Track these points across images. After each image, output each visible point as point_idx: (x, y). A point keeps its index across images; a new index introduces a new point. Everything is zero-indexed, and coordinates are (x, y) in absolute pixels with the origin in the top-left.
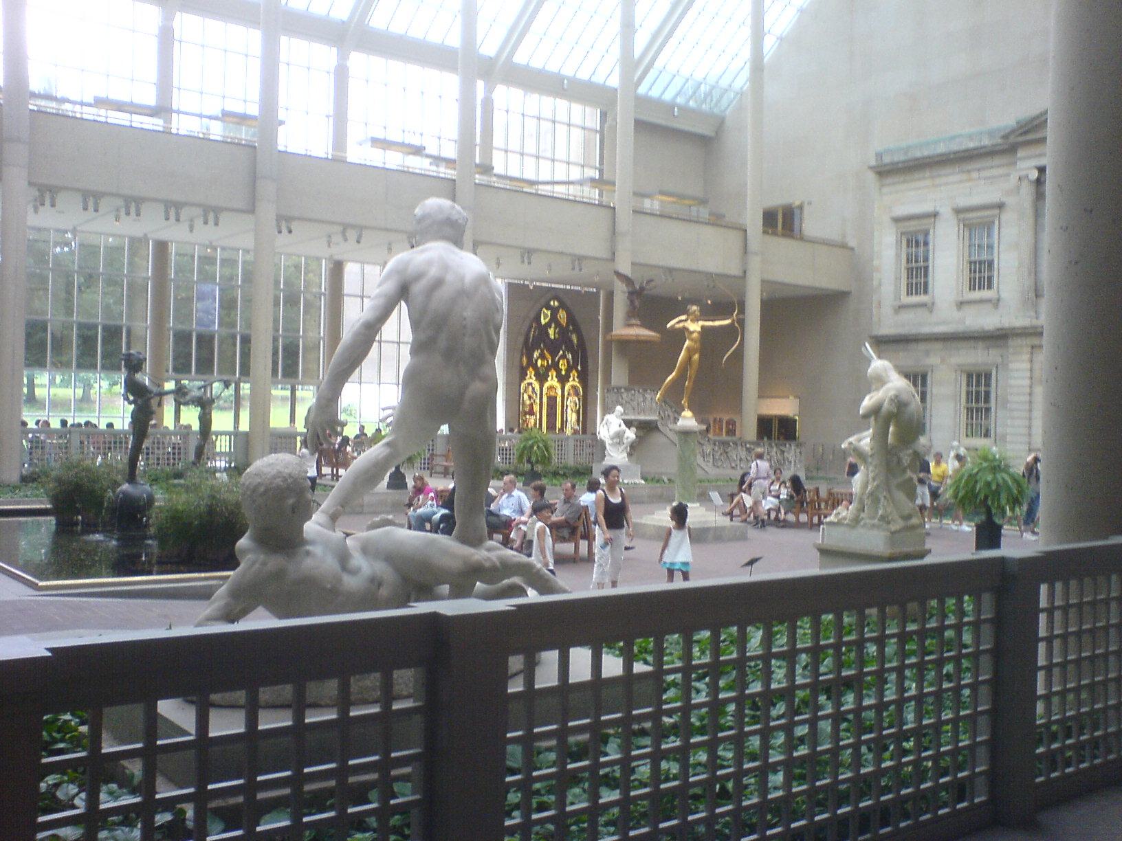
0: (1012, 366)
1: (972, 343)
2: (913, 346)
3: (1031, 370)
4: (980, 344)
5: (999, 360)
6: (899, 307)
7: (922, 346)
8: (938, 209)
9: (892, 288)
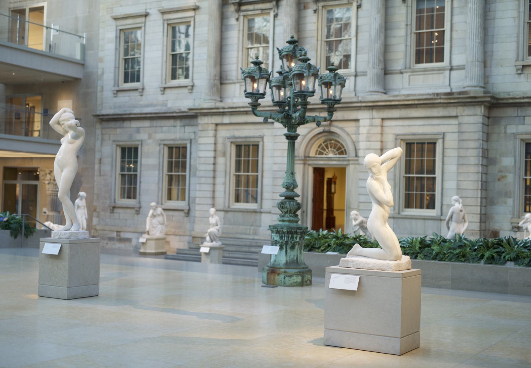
0: (201, 140)
1: (171, 122)
2: (127, 124)
3: (215, 144)
4: (178, 123)
5: (192, 136)
6: (118, 91)
7: (135, 124)
8: (148, 11)
9: (112, 76)
